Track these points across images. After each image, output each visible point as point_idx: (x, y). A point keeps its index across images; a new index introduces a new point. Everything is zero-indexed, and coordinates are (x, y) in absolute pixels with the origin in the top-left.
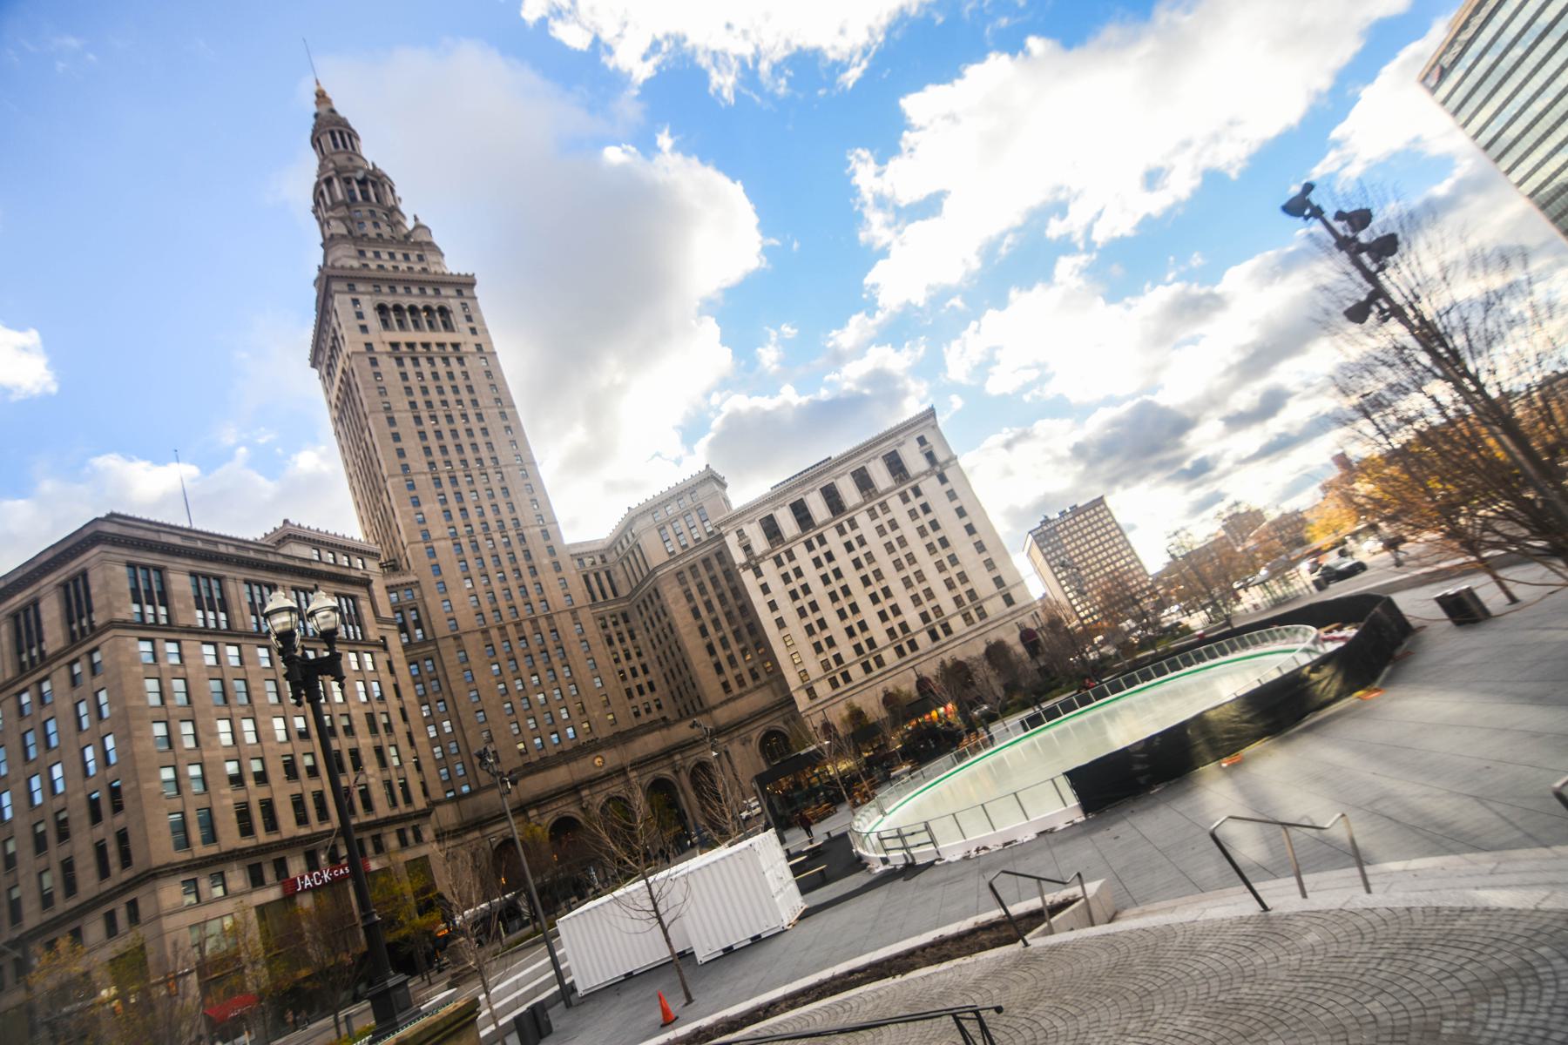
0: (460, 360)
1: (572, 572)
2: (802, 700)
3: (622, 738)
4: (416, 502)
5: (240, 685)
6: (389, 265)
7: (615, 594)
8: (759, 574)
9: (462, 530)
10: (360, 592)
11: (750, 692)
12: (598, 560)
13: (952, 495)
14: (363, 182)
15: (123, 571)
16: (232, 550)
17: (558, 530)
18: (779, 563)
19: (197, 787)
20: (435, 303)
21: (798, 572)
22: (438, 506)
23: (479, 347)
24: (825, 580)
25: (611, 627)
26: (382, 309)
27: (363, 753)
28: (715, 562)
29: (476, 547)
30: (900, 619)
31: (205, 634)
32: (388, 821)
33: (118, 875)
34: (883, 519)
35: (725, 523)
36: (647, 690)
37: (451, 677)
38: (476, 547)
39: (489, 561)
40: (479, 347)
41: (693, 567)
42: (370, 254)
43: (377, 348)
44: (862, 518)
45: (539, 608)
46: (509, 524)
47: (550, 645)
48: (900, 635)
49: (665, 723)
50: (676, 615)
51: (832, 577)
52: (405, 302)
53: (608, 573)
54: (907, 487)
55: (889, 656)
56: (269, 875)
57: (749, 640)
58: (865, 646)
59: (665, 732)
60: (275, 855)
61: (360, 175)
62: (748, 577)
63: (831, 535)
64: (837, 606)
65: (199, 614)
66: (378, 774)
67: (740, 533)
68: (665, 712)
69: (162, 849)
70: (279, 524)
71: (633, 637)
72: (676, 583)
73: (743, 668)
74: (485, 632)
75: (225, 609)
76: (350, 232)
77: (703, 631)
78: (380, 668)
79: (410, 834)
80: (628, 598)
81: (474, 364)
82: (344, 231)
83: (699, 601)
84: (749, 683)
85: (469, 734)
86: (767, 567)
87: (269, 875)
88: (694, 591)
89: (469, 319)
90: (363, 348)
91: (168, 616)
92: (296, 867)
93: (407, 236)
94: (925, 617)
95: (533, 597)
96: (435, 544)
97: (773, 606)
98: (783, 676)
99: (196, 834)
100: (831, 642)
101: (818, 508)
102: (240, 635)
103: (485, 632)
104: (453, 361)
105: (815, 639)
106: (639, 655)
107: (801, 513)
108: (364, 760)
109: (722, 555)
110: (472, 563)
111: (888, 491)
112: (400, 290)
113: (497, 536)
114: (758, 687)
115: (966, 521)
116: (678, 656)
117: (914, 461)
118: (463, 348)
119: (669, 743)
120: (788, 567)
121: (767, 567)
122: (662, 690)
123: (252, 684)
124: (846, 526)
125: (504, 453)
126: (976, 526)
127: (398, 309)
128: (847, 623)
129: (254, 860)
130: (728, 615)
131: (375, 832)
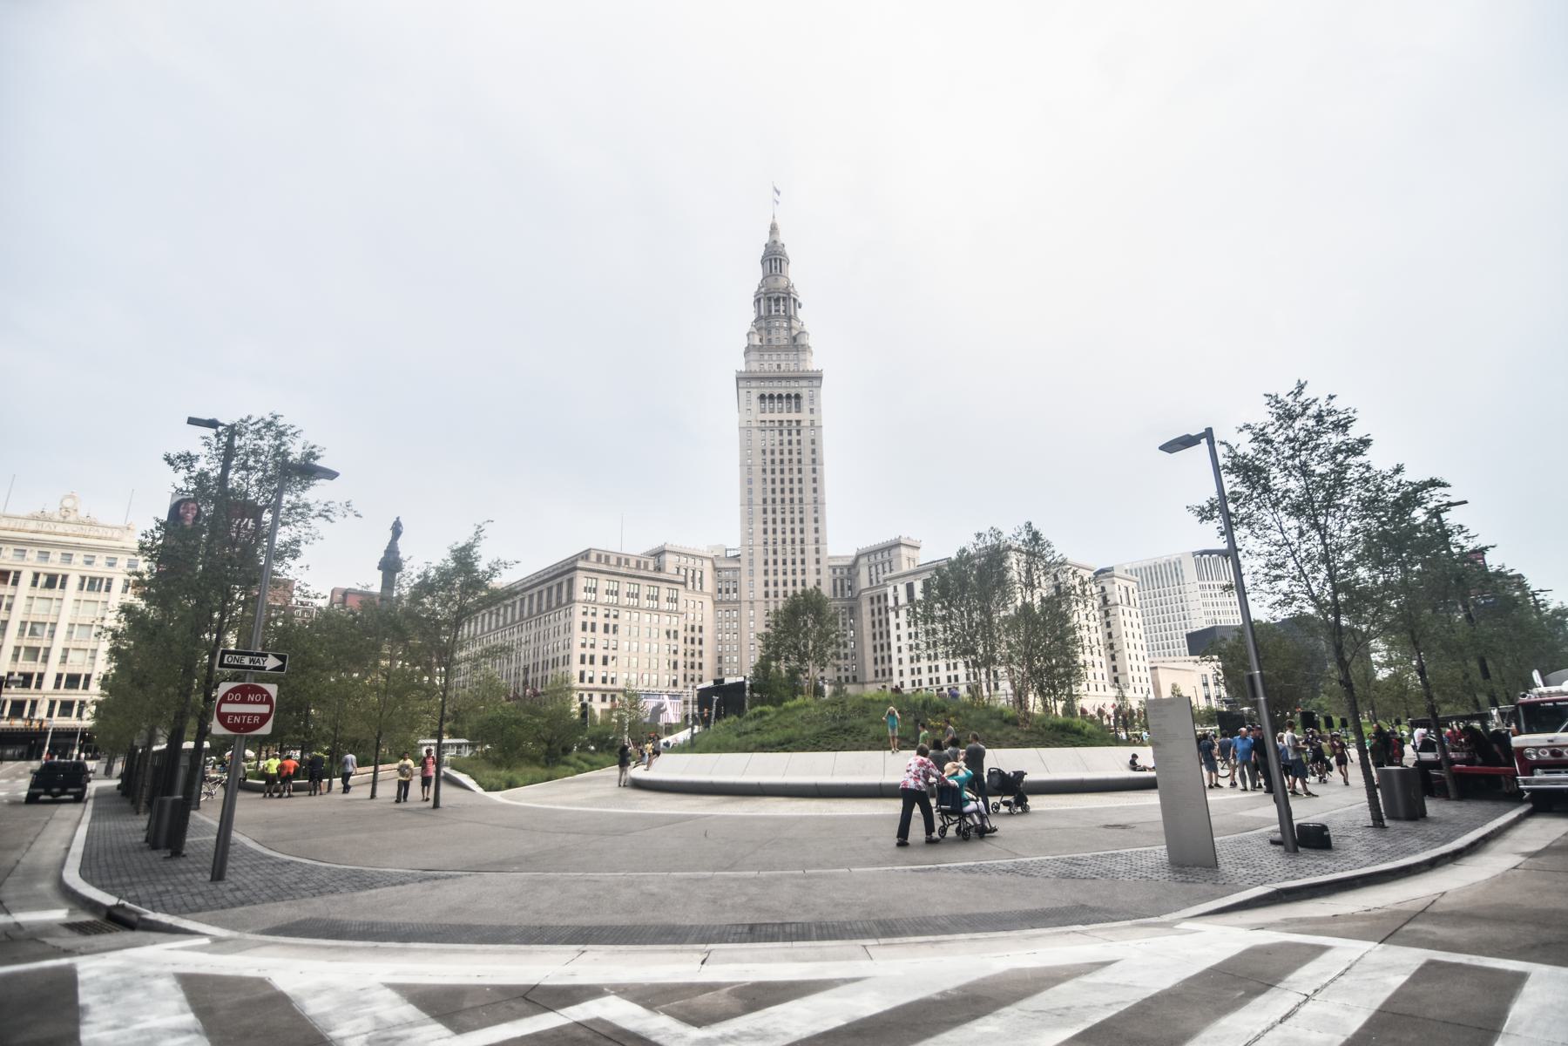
0: (799, 433)
9: (770, 541)
10: (681, 587)
22: (762, 526)
23: (812, 422)
26: (762, 397)
29: (775, 552)
38: (775, 552)
40: (812, 422)
46: (798, 541)
56: (608, 699)
81: (806, 435)
83: (876, 618)
86: (903, 613)
87: (608, 699)
89: (812, 400)
97: (899, 638)
110: (771, 562)
121: (903, 613)
125: (808, 496)
127: (771, 397)
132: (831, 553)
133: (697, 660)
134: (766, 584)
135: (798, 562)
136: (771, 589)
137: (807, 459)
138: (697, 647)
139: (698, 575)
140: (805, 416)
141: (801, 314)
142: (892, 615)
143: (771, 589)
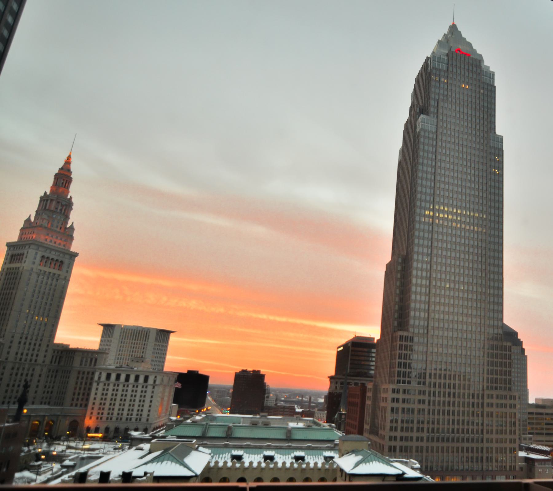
0: (57, 280)
1: (49, 355)
20: (60, 259)
35: (99, 369)
57: (85, 397)
67: (100, 373)
73: (79, 402)
88: (80, 378)
104: (55, 280)
109: (93, 373)
121: (101, 385)
128: (110, 407)
135: (37, 345)
142: (95, 385)
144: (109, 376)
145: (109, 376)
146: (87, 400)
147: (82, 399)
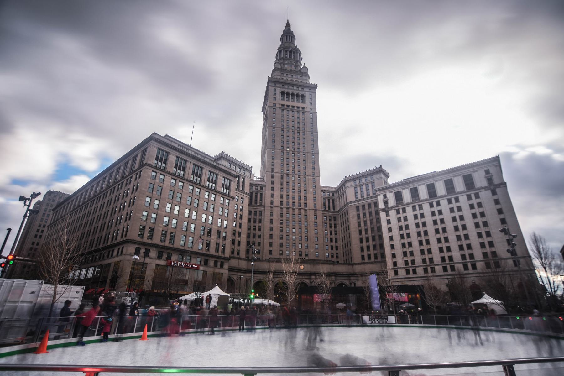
0: (303, 113)
1: (319, 195)
2: (391, 274)
3: (315, 262)
4: (273, 159)
5: (179, 195)
6: (289, 79)
7: (334, 209)
8: (388, 214)
9: (285, 171)
11: (372, 263)
12: (331, 195)
13: (497, 202)
14: (290, 52)
15: (156, 150)
16: (193, 153)
17: (319, 180)
18: (398, 212)
19: (153, 221)
20: (300, 93)
21: (406, 219)
22: (280, 162)
24: (417, 225)
25: (328, 221)
26: (282, 93)
27: (212, 231)
28: (373, 206)
30: (450, 254)
31: (174, 176)
32: (212, 256)
33: (124, 239)
34: (454, 205)
35: (380, 190)
36: (334, 248)
37: (266, 220)
39: (291, 184)
41: (363, 206)
42: (285, 75)
43: (277, 105)
44: (444, 202)
45: (303, 205)
46: (302, 173)
47: (303, 220)
48: (447, 261)
49: (333, 263)
50: (351, 223)
51: (421, 225)
52: (291, 92)
53: (333, 200)
54: (472, 194)
55: (439, 269)
56: (165, 256)
57: (377, 242)
58: (428, 260)
59: (332, 266)
60: (169, 251)
61: (290, 49)
62: (383, 215)
63: (426, 206)
64: (419, 239)
65: (175, 170)
66: (215, 240)
67: (385, 196)
68: (339, 260)
69: (134, 234)
70: (220, 153)
71: (335, 227)
72: (355, 210)
73: (372, 252)
74: (282, 208)
75: (184, 170)
76: (281, 68)
77: (360, 232)
78: (230, 205)
79: (219, 264)
80: (338, 212)
81: (308, 116)
82: (280, 67)
84: (373, 259)
85: (265, 241)
86: (393, 213)
88: (361, 215)
89: (311, 99)
90: (272, 105)
91: (165, 167)
92: (174, 257)
93: (300, 71)
94: (463, 257)
95: (303, 201)
96: (275, 174)
98: (385, 262)
99: (146, 234)
100: (412, 253)
101: (423, 193)
102: (185, 180)
103: (282, 208)
104: (301, 113)
105: (405, 250)
106: (336, 234)
107: (415, 193)
108: (212, 233)
109: (376, 204)
111: (461, 192)
112: (290, 87)
113: (296, 176)
114: (375, 262)
115: (502, 216)
116: (348, 240)
117: (480, 180)
118: (305, 110)
119: (332, 271)
120: (402, 215)
121: (393, 213)
122: (341, 251)
123: (183, 196)
124: (435, 204)
125: (309, 149)
126: (508, 220)
127: (288, 94)
128: (422, 248)
129: (162, 250)
130: (372, 229)
131: (207, 258)
132: (321, 185)
133: (237, 239)
134: (282, 197)
136: (285, 200)
137: (308, 128)
138: (238, 229)
139: (241, 180)
140: (307, 105)
141: (302, 62)
143: (285, 200)
144: (399, 197)
145: (399, 197)
146: (382, 246)
147: (375, 246)
